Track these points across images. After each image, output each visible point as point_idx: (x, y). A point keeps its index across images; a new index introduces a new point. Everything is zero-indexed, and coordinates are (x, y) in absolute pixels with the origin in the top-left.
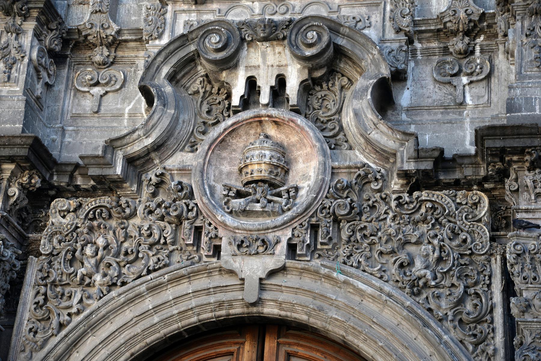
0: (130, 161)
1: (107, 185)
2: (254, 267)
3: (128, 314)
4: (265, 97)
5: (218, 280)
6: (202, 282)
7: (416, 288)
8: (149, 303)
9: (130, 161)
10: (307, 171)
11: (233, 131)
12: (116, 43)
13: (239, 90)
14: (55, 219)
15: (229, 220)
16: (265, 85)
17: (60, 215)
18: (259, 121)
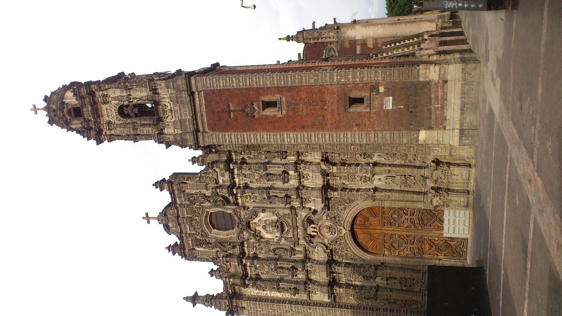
0: (327, 249)
1: (331, 250)
2: (344, 231)
3: (351, 248)
4: (315, 230)
5: (346, 236)
6: (346, 238)
7: (345, 208)
8: (350, 245)
9: (327, 249)
10: (328, 223)
11: (321, 234)
12: (306, 251)
13: (314, 234)
14: (337, 258)
15: (336, 235)
16: (313, 230)
17: (336, 258)
18: (320, 230)
